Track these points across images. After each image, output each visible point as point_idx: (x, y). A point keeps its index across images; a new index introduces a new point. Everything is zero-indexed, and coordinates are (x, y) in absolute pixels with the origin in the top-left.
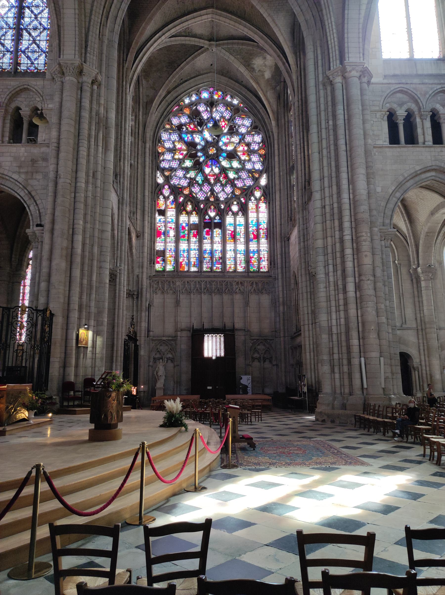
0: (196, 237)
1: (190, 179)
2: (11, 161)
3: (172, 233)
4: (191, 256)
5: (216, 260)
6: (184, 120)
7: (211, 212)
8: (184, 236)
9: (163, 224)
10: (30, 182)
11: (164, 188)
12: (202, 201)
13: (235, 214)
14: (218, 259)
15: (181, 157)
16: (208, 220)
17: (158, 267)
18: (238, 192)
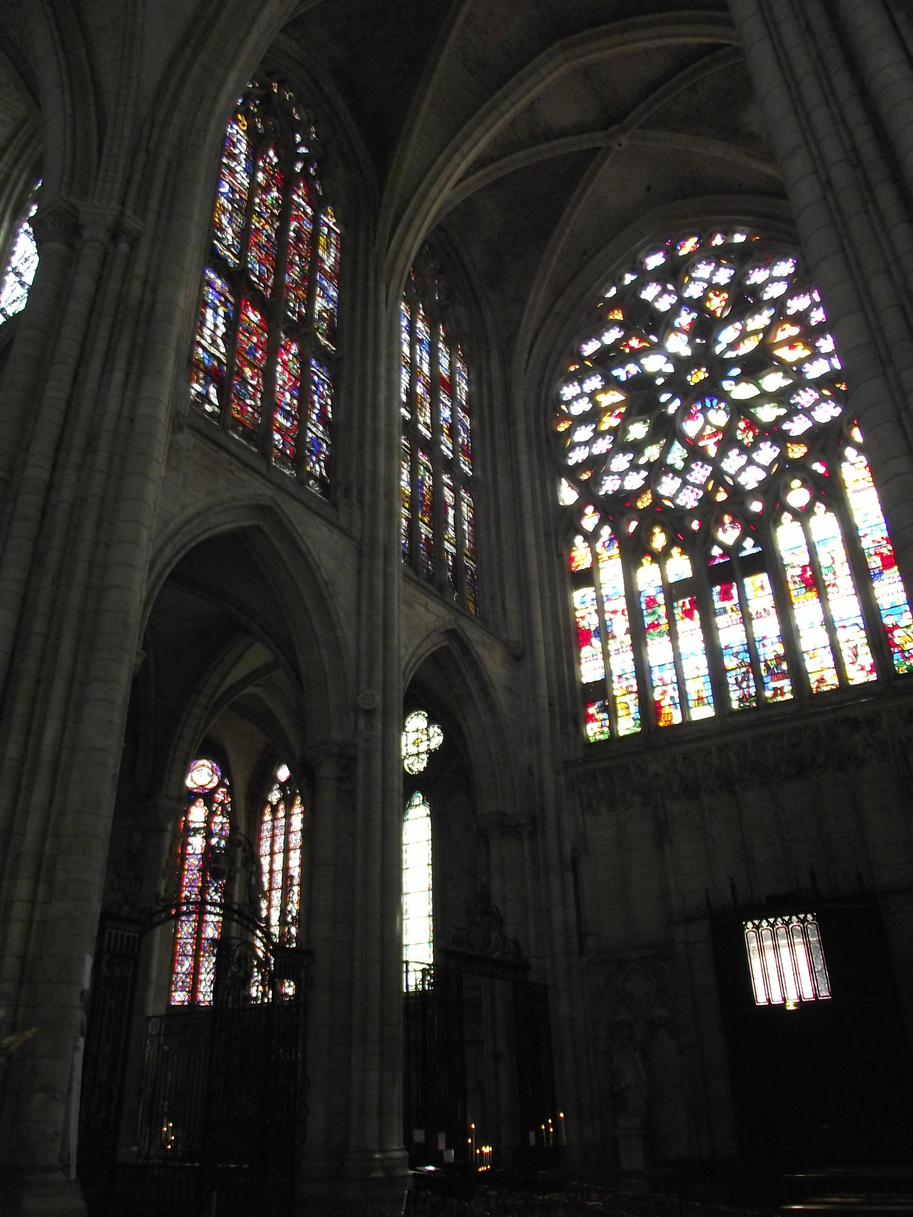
1: (649, 466)
3: (620, 625)
5: (767, 666)
6: (612, 336)
7: (725, 531)
8: (654, 626)
11: (582, 514)
12: (693, 509)
13: (803, 515)
14: (772, 664)
16: (722, 556)
17: (594, 731)
18: (797, 452)
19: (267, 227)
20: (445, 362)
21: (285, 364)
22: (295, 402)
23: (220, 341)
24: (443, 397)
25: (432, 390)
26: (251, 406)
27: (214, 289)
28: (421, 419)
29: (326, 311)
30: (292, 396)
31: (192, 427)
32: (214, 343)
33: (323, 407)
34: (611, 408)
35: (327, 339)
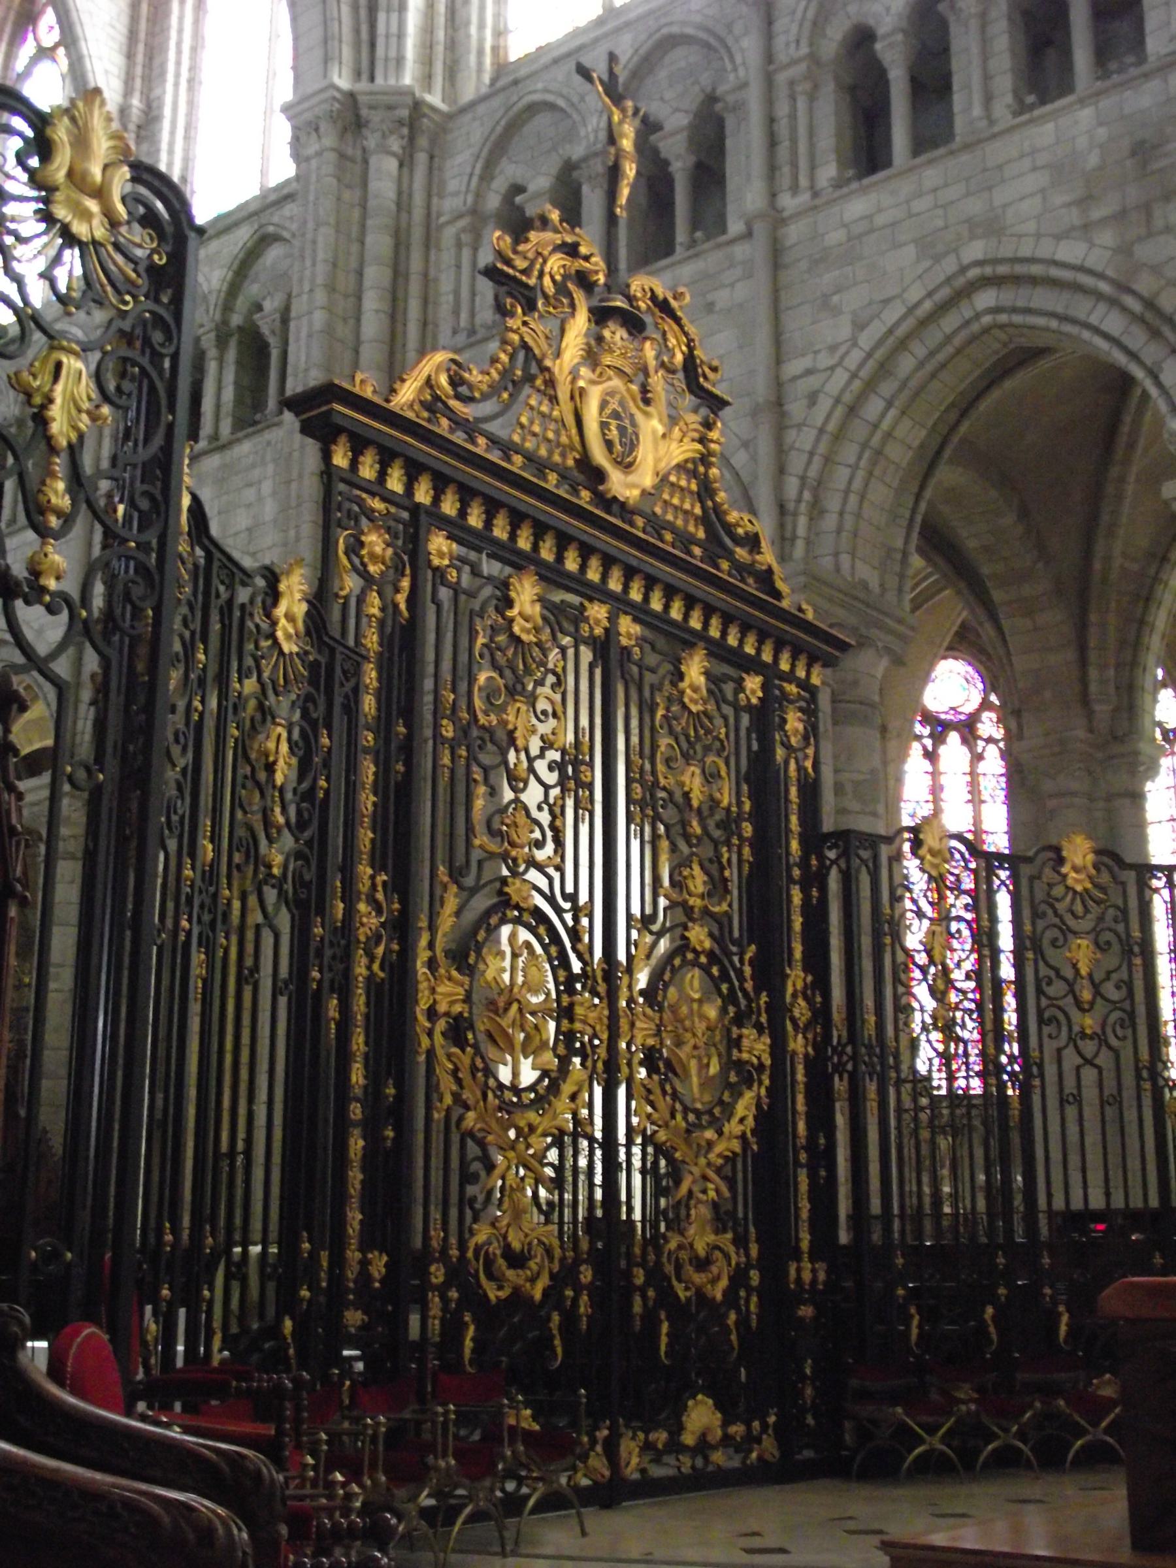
2: (1043, 191)
10: (1146, 252)
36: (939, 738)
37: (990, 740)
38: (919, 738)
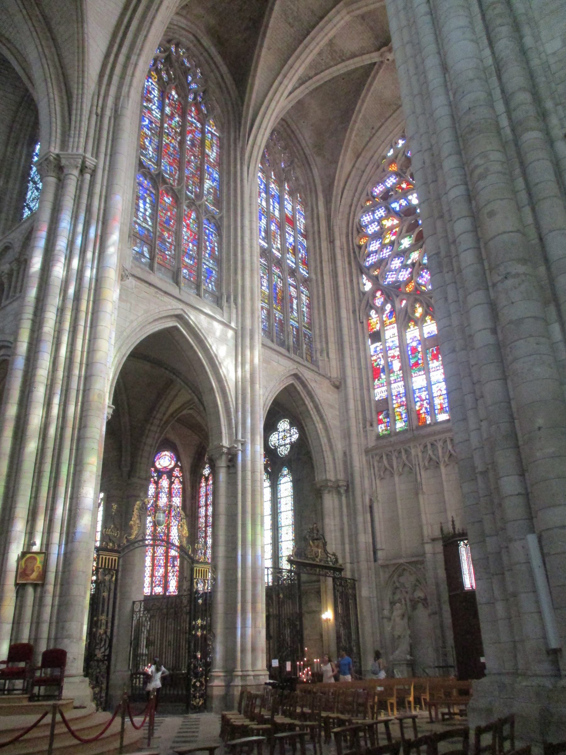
0: (437, 360)
1: (413, 264)
3: (396, 365)
4: (434, 395)
6: (391, 181)
9: (380, 355)
11: (374, 297)
15: (393, 238)
17: (381, 428)
19: (173, 141)
20: (289, 207)
21: (188, 225)
22: (195, 248)
23: (148, 219)
24: (288, 229)
25: (281, 227)
26: (169, 255)
27: (143, 187)
28: (274, 246)
29: (212, 188)
30: (193, 245)
31: (133, 276)
32: (145, 219)
33: (213, 249)
34: (391, 229)
35: (213, 206)
36: (160, 477)
37: (177, 477)
38: (153, 477)
